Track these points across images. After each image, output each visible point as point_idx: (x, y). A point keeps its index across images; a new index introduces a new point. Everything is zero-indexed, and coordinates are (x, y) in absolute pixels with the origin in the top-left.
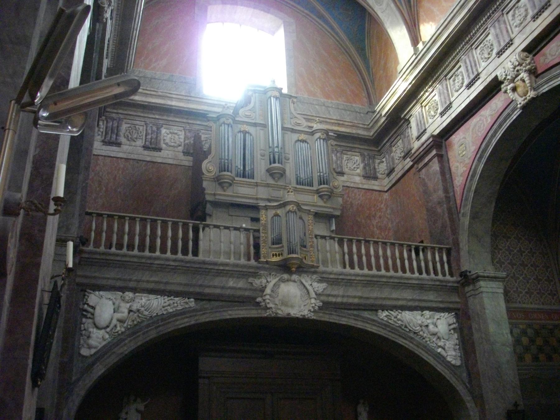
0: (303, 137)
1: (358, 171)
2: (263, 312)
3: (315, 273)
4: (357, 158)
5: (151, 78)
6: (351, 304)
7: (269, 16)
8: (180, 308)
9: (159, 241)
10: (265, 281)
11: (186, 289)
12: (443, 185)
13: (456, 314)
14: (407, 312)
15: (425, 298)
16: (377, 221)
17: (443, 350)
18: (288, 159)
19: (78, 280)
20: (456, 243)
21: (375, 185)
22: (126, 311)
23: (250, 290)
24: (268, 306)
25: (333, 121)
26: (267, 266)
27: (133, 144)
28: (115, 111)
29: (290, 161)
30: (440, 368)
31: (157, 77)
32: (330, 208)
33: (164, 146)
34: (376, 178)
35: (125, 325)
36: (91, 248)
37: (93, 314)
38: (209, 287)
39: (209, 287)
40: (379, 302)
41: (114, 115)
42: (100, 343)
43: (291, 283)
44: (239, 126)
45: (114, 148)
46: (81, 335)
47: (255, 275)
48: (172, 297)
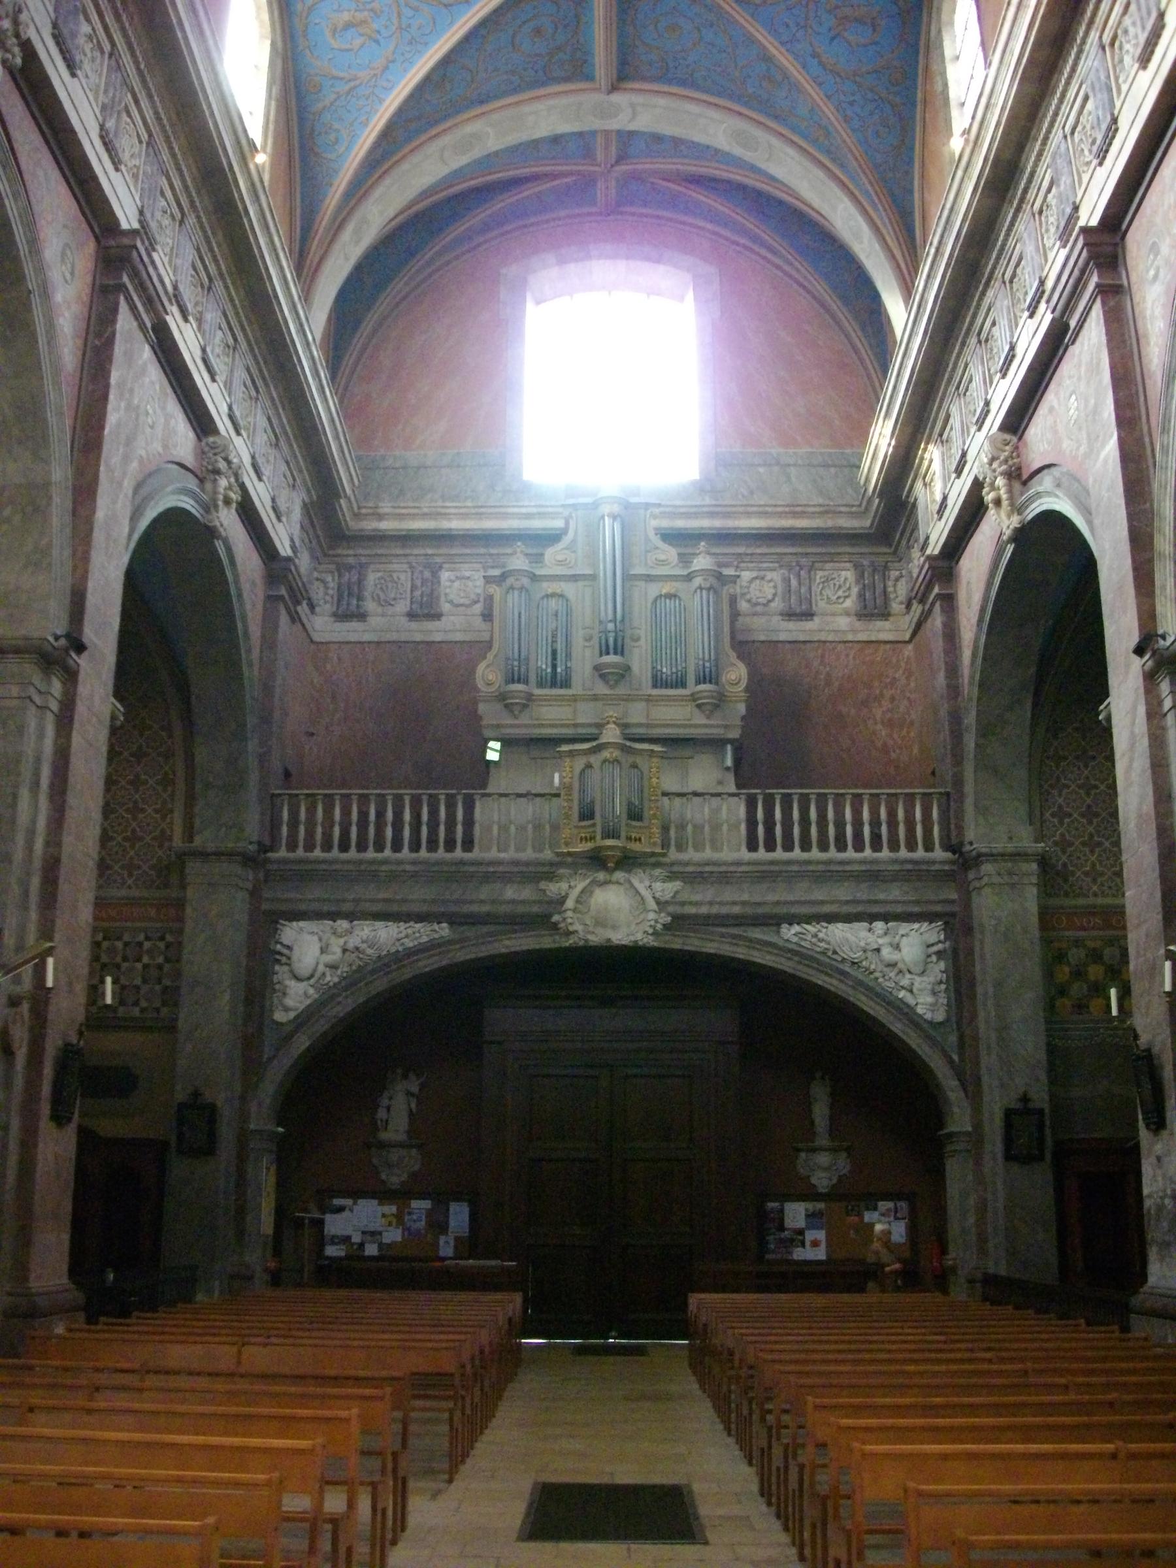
1: (848, 603)
5: (419, 468)
6: (727, 916)
7: (661, 268)
8: (425, 939)
11: (435, 909)
12: (946, 663)
13: (946, 923)
14: (840, 925)
15: (882, 896)
16: (885, 709)
17: (908, 994)
18: (638, 639)
19: (265, 906)
20: (958, 782)
21: (883, 630)
22: (339, 951)
23: (540, 902)
24: (571, 928)
25: (780, 509)
26: (569, 859)
27: (390, 610)
29: (642, 642)
30: (897, 1027)
32: (718, 726)
33: (446, 607)
34: (885, 615)
35: (339, 972)
36: (282, 853)
37: (289, 958)
39: (471, 902)
40: (784, 910)
41: (351, 560)
42: (301, 1002)
45: (354, 625)
46: (274, 991)
47: (551, 877)
48: (412, 923)
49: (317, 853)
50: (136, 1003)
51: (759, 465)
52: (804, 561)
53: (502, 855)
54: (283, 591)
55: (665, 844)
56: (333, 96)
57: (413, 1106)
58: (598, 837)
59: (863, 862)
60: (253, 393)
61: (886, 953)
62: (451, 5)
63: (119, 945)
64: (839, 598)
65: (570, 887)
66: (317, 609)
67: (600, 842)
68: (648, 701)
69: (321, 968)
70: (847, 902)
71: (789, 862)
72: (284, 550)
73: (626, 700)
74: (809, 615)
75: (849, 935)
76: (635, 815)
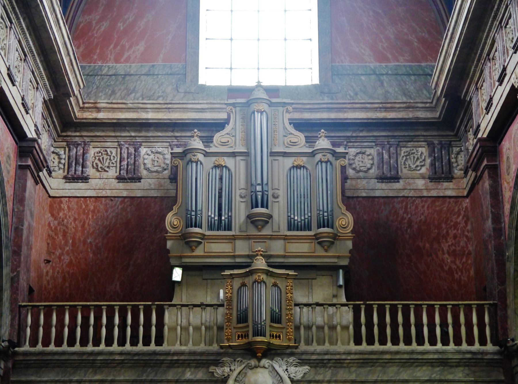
0: (301, 161)
1: (423, 170)
3: (292, 354)
4: (423, 150)
5: (125, 75)
9: (104, 331)
10: (228, 369)
16: (450, 243)
20: (503, 296)
21: (448, 189)
25: (376, 106)
26: (230, 351)
27: (105, 175)
28: (78, 134)
29: (280, 199)
31: (132, 72)
33: (144, 173)
34: (449, 177)
41: (77, 139)
43: (259, 370)
44: (214, 159)
45: (80, 185)
47: (217, 363)
49: (52, 347)
51: (362, 75)
52: (392, 141)
53: (183, 348)
54: (30, 163)
55: (297, 340)
59: (437, 352)
64: (417, 166)
66: (53, 174)
67: (251, 338)
68: (284, 239)
71: (383, 353)
72: (31, 133)
73: (270, 239)
74: (396, 178)
76: (276, 319)
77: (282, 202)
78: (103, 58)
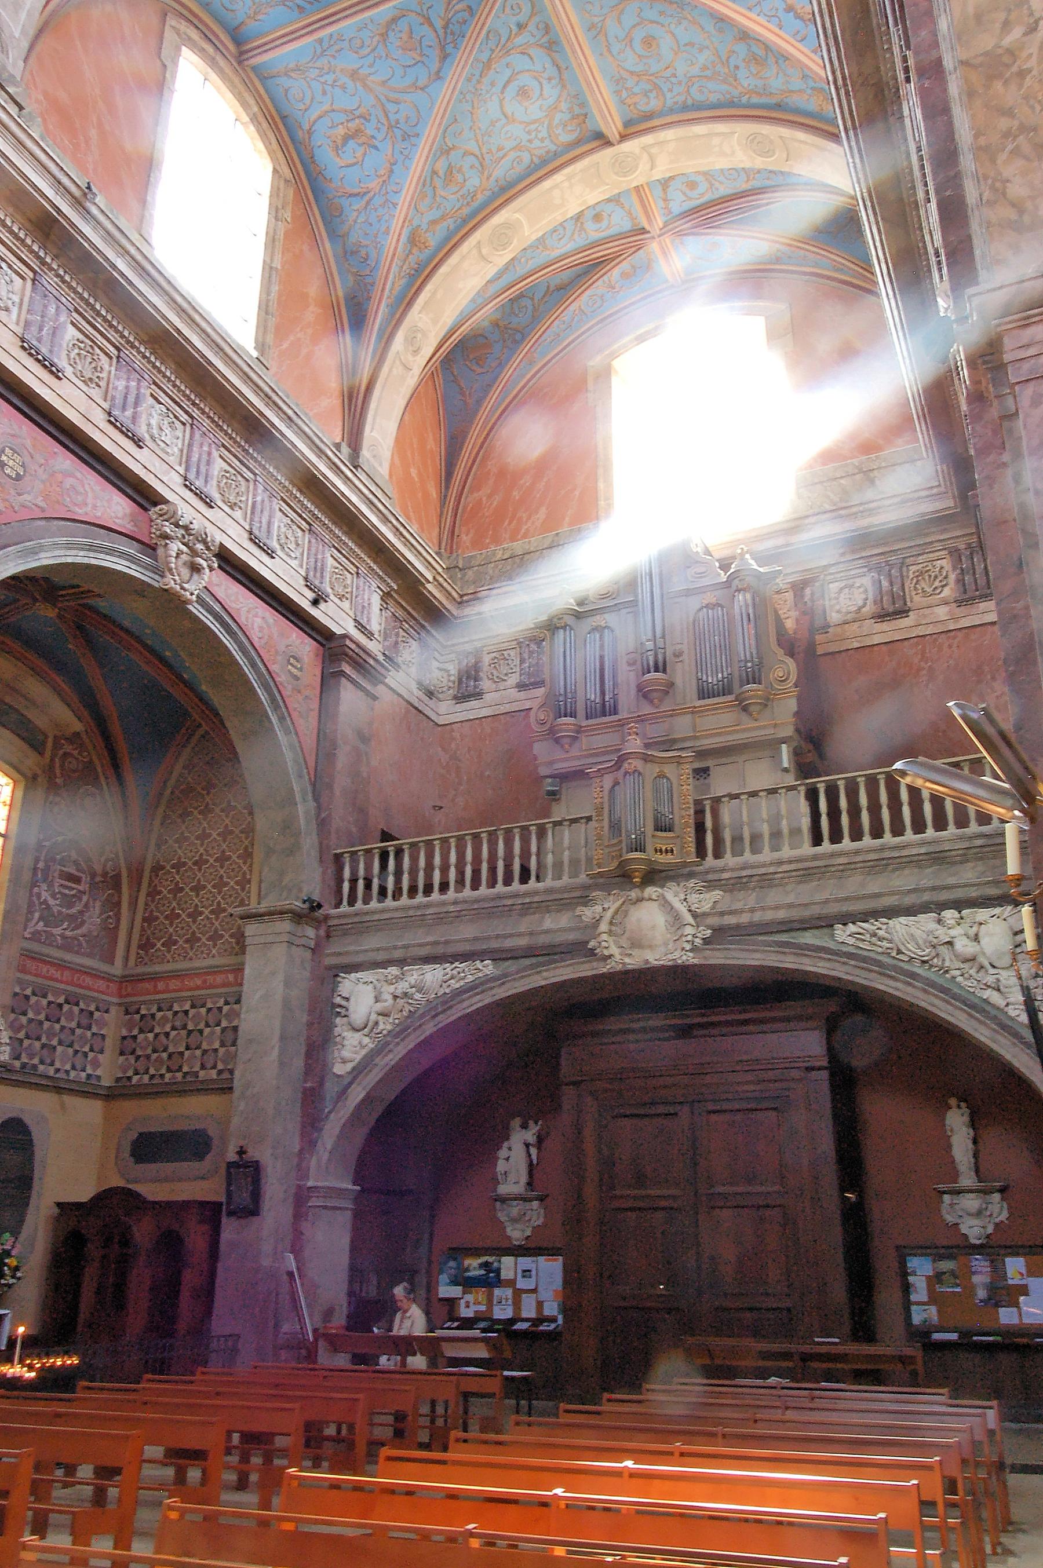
1: (947, 592)
2: (602, 964)
3: (691, 875)
4: (944, 563)
6: (772, 923)
8: (470, 978)
10: (601, 908)
14: (902, 919)
15: (951, 881)
22: (389, 998)
24: (606, 953)
26: (601, 880)
29: (685, 657)
31: (532, 549)
37: (347, 1010)
38: (511, 935)
40: (834, 909)
43: (645, 904)
45: (474, 704)
46: (336, 1044)
47: (585, 901)
48: (457, 964)
50: (214, 1067)
51: (842, 477)
55: (701, 852)
56: (355, 214)
57: (534, 1157)
58: (624, 850)
60: (249, 475)
61: (964, 946)
62: (426, 87)
63: (203, 1011)
64: (936, 588)
65: (604, 907)
68: (692, 712)
69: (374, 1017)
70: (910, 891)
75: (913, 930)
77: (687, 661)
78: (497, 540)
